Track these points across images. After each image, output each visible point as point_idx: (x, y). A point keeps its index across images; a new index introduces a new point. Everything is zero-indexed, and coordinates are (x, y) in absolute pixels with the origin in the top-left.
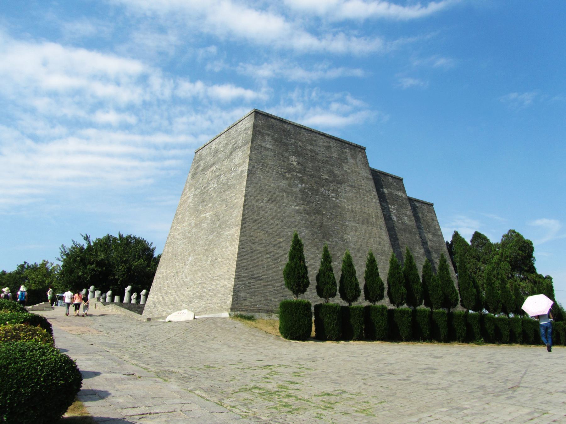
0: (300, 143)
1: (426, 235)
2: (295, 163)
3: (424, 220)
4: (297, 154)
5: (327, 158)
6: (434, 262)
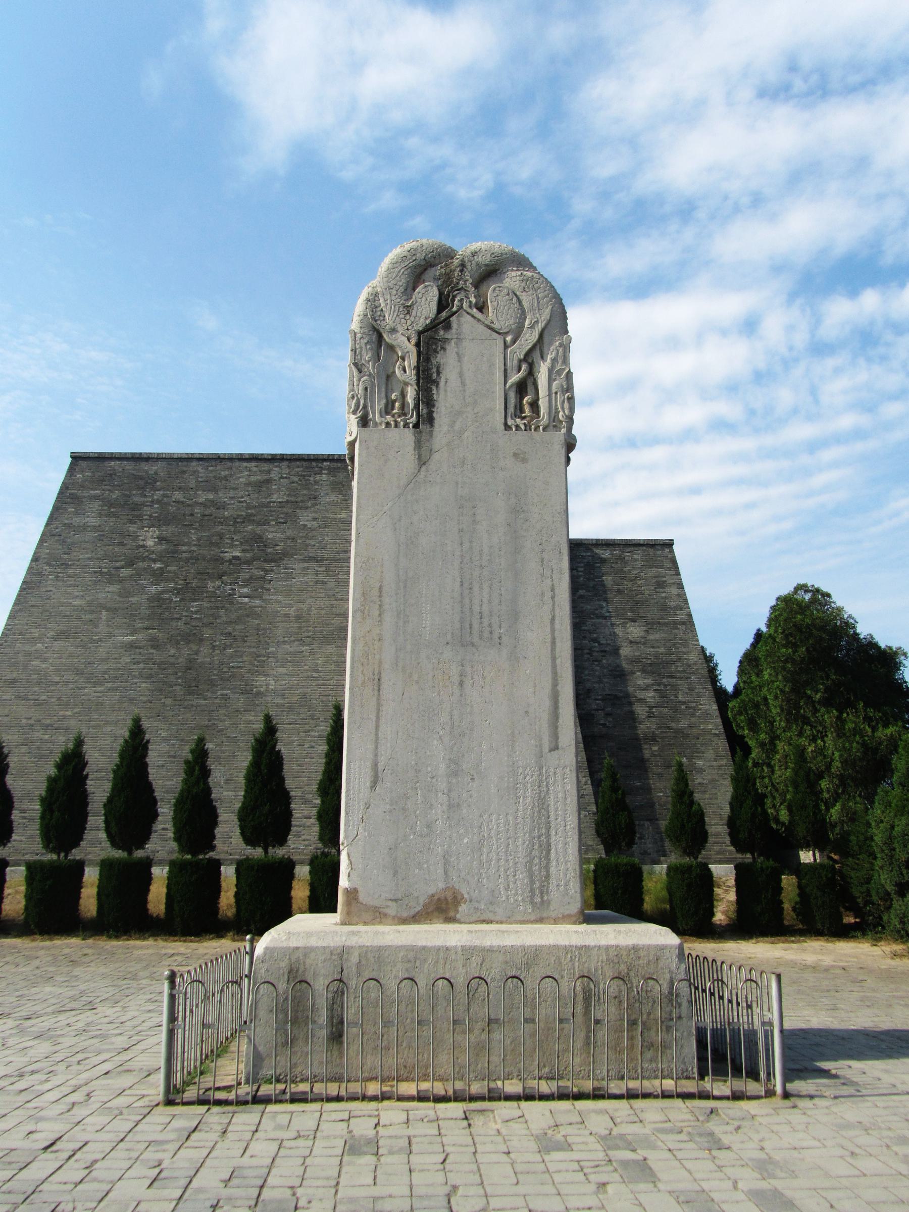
0: (178, 495)
1: (619, 631)
2: (150, 543)
3: (619, 591)
4: (158, 521)
5: (250, 509)
6: (633, 700)
